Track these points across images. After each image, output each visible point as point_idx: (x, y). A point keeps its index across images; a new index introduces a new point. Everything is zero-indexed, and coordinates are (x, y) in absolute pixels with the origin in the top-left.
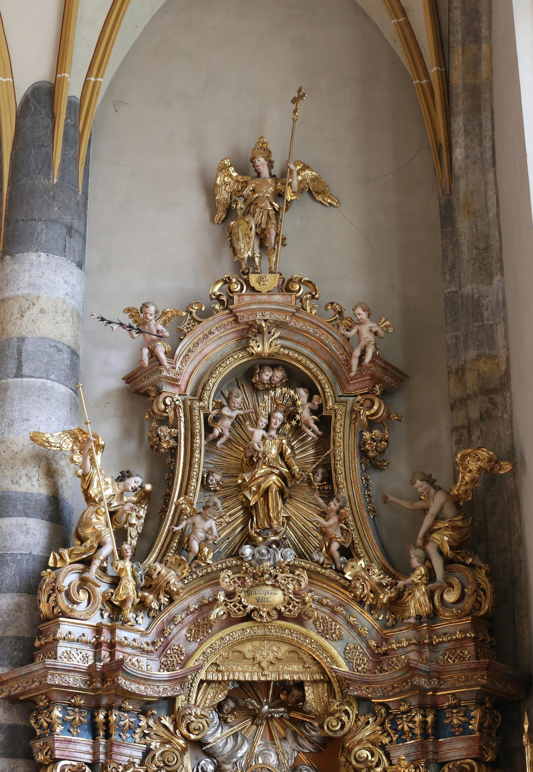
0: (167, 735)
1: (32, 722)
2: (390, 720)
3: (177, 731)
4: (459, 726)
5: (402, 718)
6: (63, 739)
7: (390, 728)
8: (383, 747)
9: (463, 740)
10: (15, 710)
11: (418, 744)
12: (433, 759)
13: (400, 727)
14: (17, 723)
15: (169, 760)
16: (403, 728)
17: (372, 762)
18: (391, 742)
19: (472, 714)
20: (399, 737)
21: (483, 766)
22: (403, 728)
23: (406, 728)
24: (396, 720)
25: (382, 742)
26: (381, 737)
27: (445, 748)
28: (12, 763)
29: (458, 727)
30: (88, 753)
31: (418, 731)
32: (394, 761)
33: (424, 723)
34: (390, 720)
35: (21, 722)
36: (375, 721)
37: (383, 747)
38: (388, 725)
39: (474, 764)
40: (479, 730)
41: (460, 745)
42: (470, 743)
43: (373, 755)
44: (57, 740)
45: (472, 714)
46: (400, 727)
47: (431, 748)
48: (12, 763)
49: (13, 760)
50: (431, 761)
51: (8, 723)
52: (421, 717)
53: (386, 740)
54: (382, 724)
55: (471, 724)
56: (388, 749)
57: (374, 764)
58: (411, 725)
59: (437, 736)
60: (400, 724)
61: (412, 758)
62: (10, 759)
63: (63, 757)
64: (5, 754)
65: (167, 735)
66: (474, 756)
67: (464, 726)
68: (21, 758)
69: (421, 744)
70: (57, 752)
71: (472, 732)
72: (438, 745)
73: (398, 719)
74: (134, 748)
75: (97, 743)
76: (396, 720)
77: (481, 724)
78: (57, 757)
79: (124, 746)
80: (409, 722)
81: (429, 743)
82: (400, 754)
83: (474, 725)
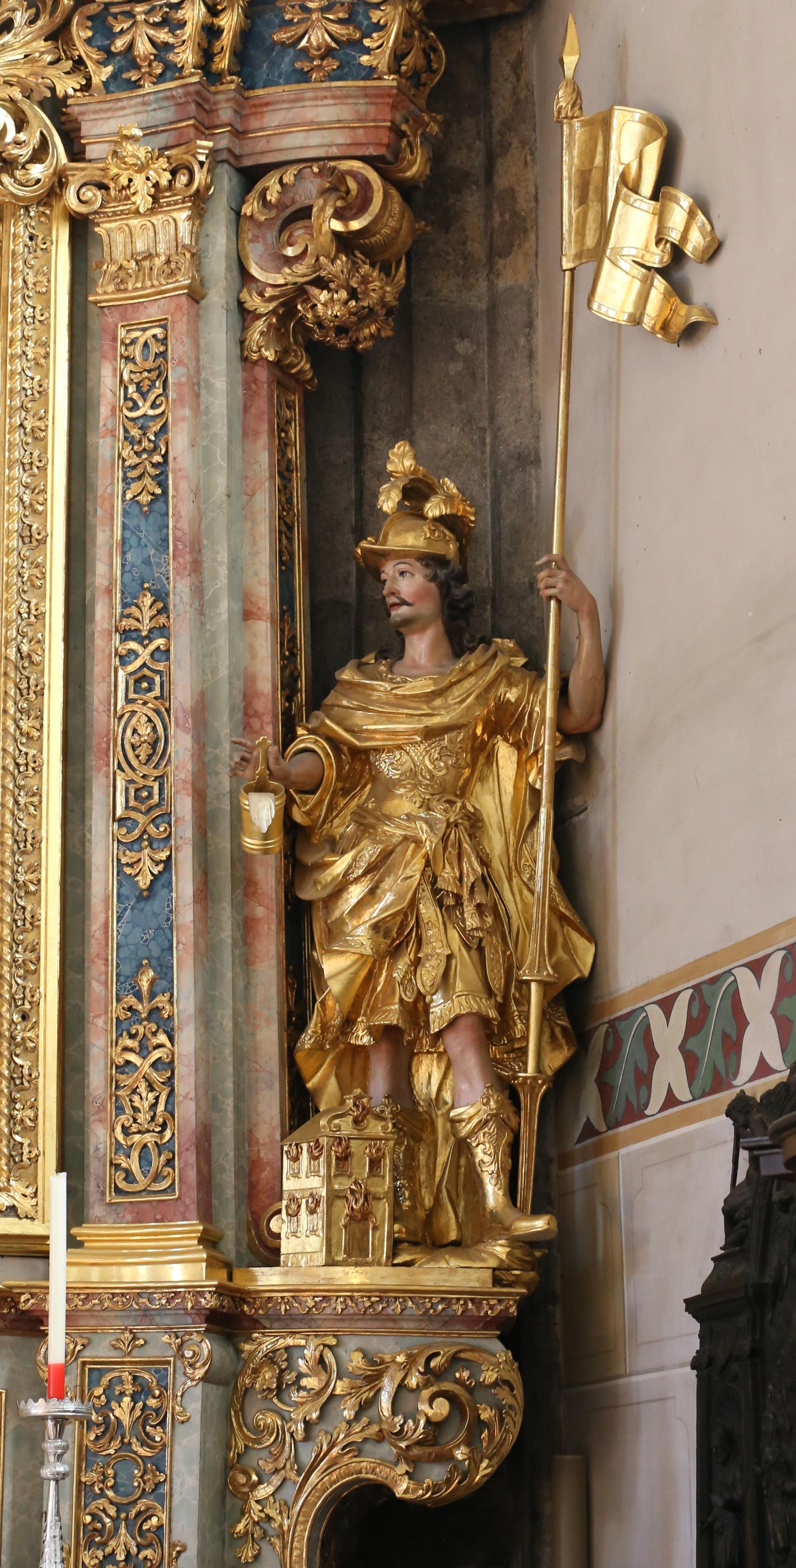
2: (90, 18)
4: (329, 52)
5: (131, 15)
7: (89, 41)
8: (55, 106)
9: (341, 98)
11: (187, 94)
12: (229, 150)
13: (120, 44)
16: (131, 46)
17: (17, 143)
18: (87, 87)
19: (375, 16)
20: (114, 76)
21: (393, 192)
22: (131, 46)
23: (143, 47)
24: (110, 19)
25: (53, 90)
26: (51, 72)
27: (273, 119)
29: (322, 58)
31: (186, 56)
32: (92, 152)
33: (211, 32)
34: (90, 18)
36: (32, 22)
37: (55, 106)
38: (80, 33)
39: (373, 177)
40: (395, 67)
41: (327, 112)
42: (362, 109)
43: (19, 129)
45: (375, 16)
46: (120, 44)
47: (225, 114)
50: (225, 156)
52: (203, 9)
53: (67, 85)
54: (59, 35)
55: (368, 51)
56: (76, 109)
57: (25, 153)
58: (163, 36)
59: (248, 84)
60: (122, 32)
61: (162, 140)
66: (371, 151)
67: (343, 58)
69: (198, 93)
71: (370, 72)
72: (245, 107)
73: (115, 16)
76: (110, 19)
77: (398, 57)
80: (155, 25)
81: (221, 97)
82: (122, 127)
83: (378, 52)
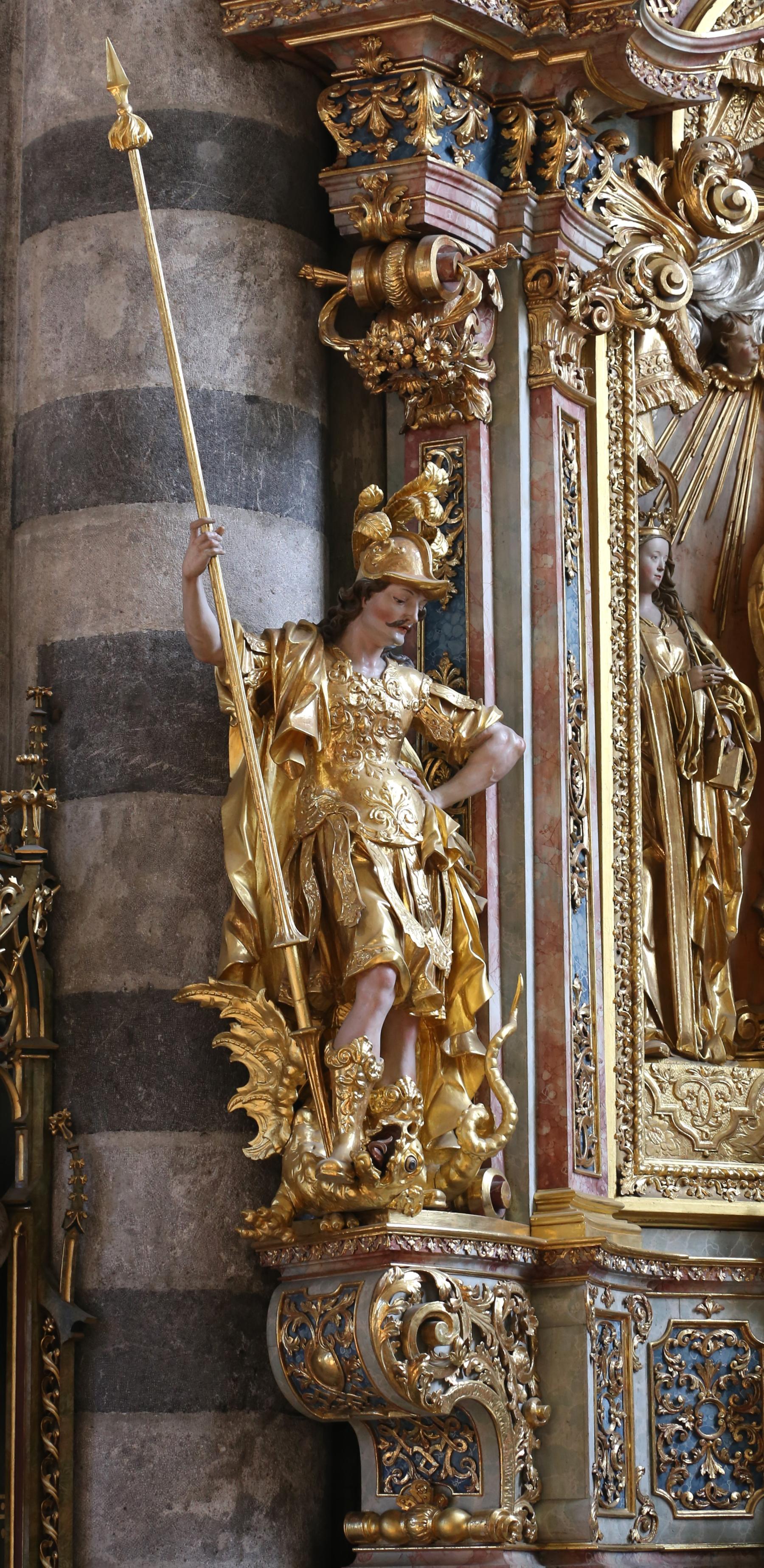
0: (651, 213)
1: (326, 115)
3: (680, 204)
6: (447, 172)
10: (251, 78)
14: (259, 118)
15: (674, 279)
28: (250, 231)
30: (486, 223)
35: (267, 117)
44: (434, 172)
48: (250, 231)
49: (251, 224)
51: (237, 112)
62: (242, 219)
63: (440, 225)
64: (230, 201)
65: (651, 213)
68: (271, 221)
70: (429, 207)
74: (592, 233)
75: (516, 201)
78: (428, 220)
79: (577, 222)
